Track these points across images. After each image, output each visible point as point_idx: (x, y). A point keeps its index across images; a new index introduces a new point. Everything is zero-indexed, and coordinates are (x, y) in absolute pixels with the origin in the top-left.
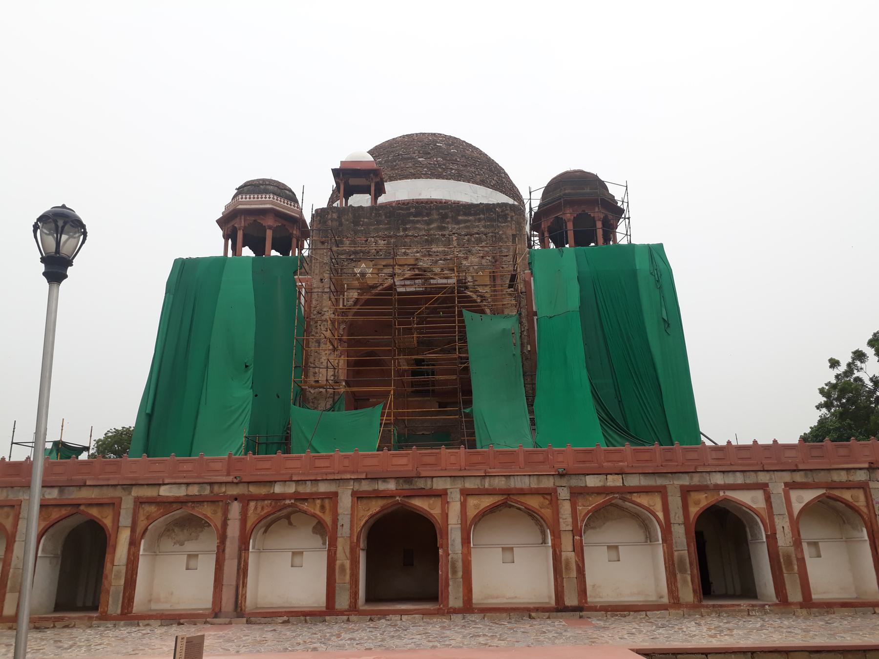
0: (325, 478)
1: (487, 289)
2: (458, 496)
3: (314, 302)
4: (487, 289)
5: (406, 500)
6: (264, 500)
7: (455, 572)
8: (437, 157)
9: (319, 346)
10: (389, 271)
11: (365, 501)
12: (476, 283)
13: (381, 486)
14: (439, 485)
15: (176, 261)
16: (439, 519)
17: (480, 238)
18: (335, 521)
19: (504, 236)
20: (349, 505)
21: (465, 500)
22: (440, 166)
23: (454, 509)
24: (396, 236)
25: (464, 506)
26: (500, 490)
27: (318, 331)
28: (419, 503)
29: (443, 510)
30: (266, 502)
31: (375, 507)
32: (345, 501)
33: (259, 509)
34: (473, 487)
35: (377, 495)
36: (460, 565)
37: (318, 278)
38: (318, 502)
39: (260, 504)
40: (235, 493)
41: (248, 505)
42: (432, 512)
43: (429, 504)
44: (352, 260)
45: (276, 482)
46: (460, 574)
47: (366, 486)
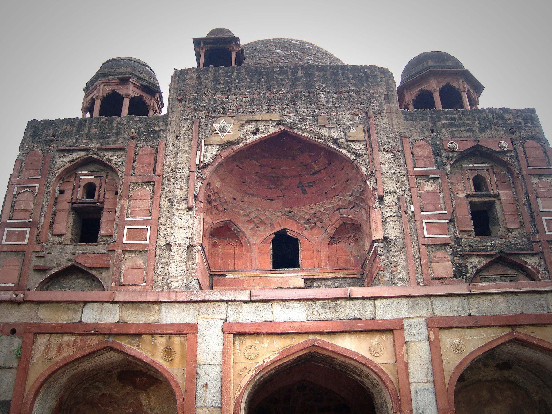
0: (173, 298)
2: (424, 331)
3: (168, 160)
4: (361, 146)
5: (325, 339)
6: (62, 334)
8: (294, 49)
9: (171, 205)
10: (252, 127)
11: (248, 342)
12: (349, 139)
15: (30, 123)
16: (389, 372)
17: (350, 95)
18: (192, 376)
19: (375, 95)
20: (219, 348)
21: (437, 338)
22: (297, 56)
24: (259, 93)
25: (435, 348)
26: (495, 318)
27: (171, 189)
28: (348, 344)
29: (396, 355)
30: (66, 338)
31: (269, 352)
33: (54, 351)
34: (449, 314)
37: (173, 135)
38: (161, 341)
39: (55, 340)
40: (12, 321)
41: (34, 341)
42: (377, 361)
43: (371, 347)
44: (211, 116)
45: (85, 303)
47: (250, 315)
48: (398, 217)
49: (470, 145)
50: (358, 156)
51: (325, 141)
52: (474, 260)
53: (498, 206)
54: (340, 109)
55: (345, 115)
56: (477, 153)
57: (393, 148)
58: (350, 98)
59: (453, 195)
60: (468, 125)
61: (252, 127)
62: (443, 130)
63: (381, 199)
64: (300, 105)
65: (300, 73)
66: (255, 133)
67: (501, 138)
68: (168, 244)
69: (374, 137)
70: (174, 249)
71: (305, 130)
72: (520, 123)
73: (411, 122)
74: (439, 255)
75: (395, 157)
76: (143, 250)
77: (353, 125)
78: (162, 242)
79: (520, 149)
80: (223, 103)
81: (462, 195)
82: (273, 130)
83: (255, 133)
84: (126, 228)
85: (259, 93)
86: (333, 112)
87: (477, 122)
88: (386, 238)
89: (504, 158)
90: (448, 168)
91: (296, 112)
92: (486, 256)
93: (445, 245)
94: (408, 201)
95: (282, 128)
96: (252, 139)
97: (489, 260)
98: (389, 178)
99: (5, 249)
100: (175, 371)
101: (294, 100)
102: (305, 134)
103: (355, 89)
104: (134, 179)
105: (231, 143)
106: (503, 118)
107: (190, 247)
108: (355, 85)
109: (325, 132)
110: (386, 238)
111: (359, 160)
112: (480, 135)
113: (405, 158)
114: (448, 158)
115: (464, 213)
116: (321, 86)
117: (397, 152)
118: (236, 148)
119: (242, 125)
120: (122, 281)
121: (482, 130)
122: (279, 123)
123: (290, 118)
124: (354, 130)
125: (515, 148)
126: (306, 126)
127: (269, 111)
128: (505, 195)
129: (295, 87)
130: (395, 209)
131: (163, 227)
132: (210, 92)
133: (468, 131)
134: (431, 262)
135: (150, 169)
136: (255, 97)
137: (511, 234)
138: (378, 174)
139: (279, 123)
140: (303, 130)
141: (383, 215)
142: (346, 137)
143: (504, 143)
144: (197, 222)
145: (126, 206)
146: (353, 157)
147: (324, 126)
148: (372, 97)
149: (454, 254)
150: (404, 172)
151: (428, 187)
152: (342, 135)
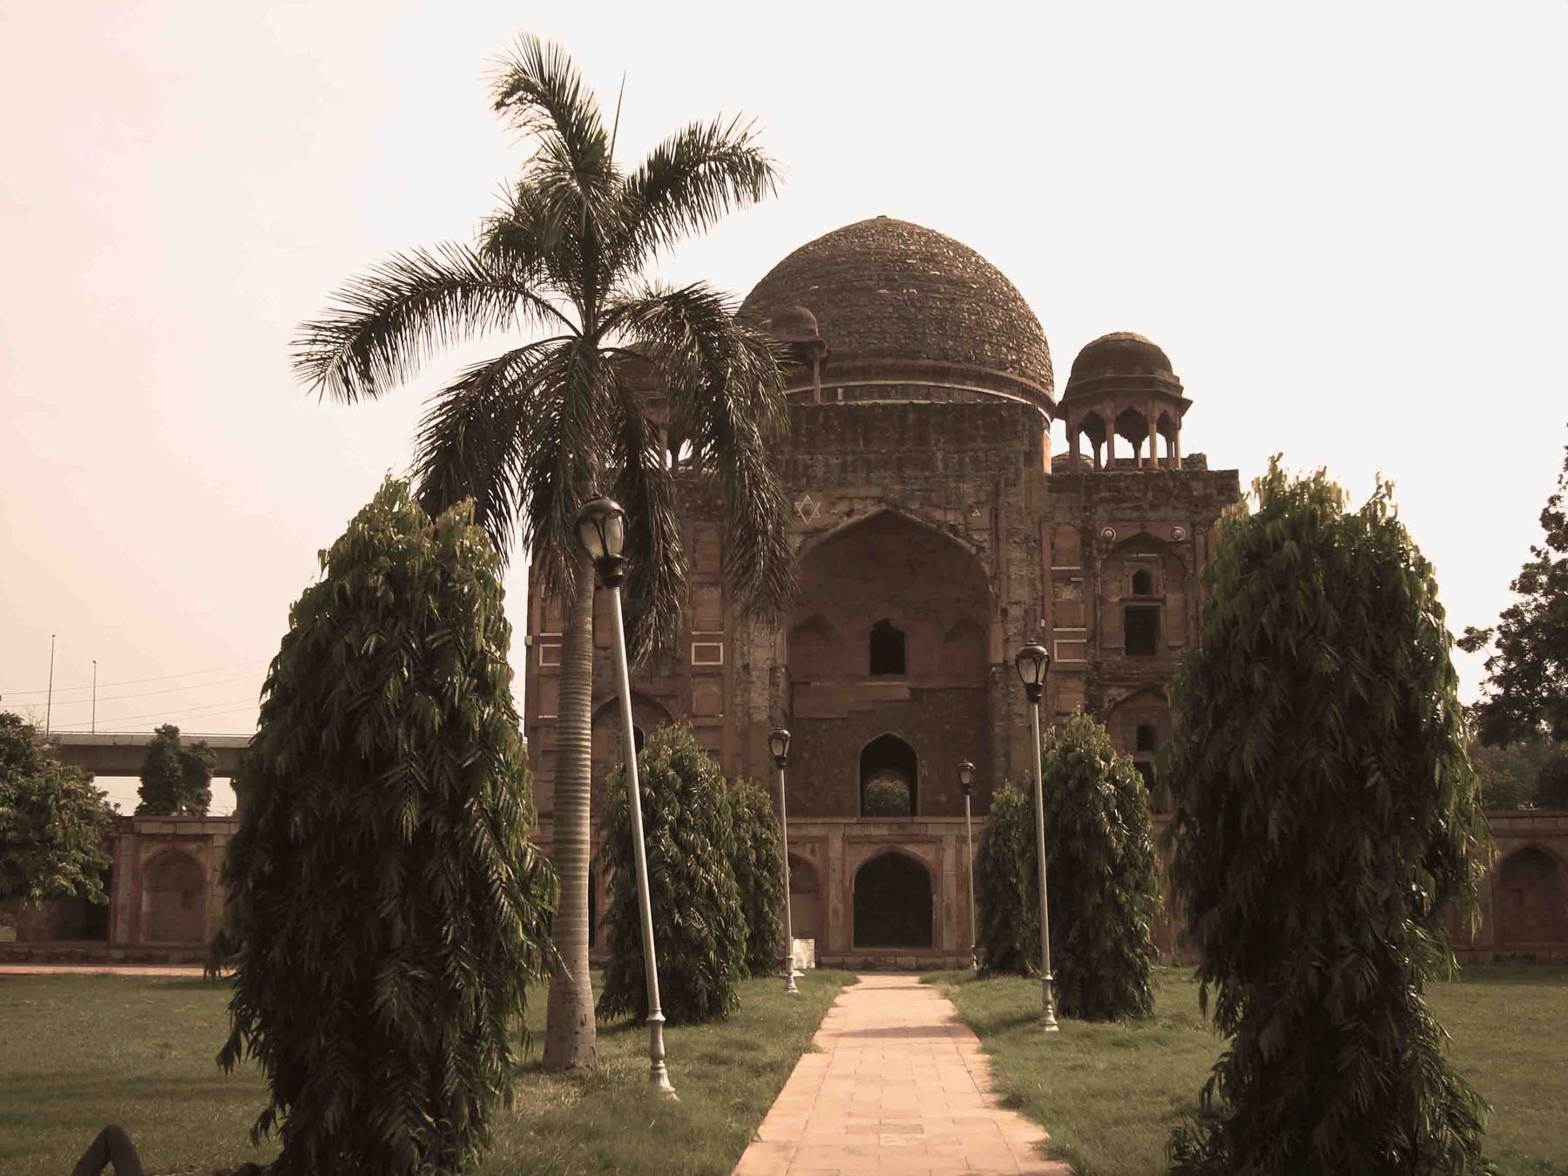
7: (949, 917)
10: (844, 506)
13: (874, 831)
14: (933, 831)
22: (913, 305)
28: (912, 849)
31: (868, 852)
32: (836, 845)
35: (869, 840)
36: (954, 908)
46: (954, 920)
48: (1024, 635)
50: (980, 549)
51: (939, 527)
52: (1113, 692)
54: (960, 478)
55: (967, 488)
56: (1143, 541)
57: (1027, 539)
58: (975, 460)
59: (1102, 600)
60: (1137, 499)
61: (844, 506)
62: (1100, 509)
63: (1005, 612)
64: (908, 472)
65: (911, 417)
66: (849, 514)
67: (1179, 522)
68: (746, 667)
69: (1003, 524)
70: (754, 674)
71: (914, 511)
73: (1055, 495)
74: (1070, 684)
75: (1030, 552)
76: (716, 673)
77: (978, 504)
78: (739, 664)
79: (1201, 539)
80: (807, 467)
81: (1115, 599)
82: (873, 510)
83: (849, 514)
85: (853, 453)
86: (953, 485)
87: (1150, 494)
88: (1006, 662)
89: (1179, 551)
91: (903, 483)
92: (1128, 687)
93: (1078, 673)
94: (1039, 613)
95: (884, 507)
97: (1132, 691)
99: (544, 672)
100: (816, 861)
101: (900, 465)
104: (697, 578)
105: (817, 531)
106: (1188, 488)
107: (773, 670)
108: (984, 439)
109: (938, 515)
110: (1006, 662)
112: (1150, 515)
113: (1041, 552)
114: (1100, 551)
115: (1114, 623)
117: (1033, 546)
118: (825, 535)
119: (833, 504)
122: (880, 500)
124: (977, 513)
126: (915, 506)
127: (868, 481)
128: (1173, 599)
130: (1020, 624)
131: (738, 644)
132: (787, 448)
133: (1136, 508)
135: (715, 564)
136: (849, 458)
137: (1173, 654)
138: (1003, 578)
139: (880, 500)
140: (911, 511)
141: (1005, 632)
142: (967, 524)
143: (1179, 531)
144: (779, 639)
145: (690, 613)
146: (974, 550)
147: (939, 506)
148: (1007, 458)
149: (1089, 683)
150: (1037, 573)
151: (1068, 594)
152: (961, 520)
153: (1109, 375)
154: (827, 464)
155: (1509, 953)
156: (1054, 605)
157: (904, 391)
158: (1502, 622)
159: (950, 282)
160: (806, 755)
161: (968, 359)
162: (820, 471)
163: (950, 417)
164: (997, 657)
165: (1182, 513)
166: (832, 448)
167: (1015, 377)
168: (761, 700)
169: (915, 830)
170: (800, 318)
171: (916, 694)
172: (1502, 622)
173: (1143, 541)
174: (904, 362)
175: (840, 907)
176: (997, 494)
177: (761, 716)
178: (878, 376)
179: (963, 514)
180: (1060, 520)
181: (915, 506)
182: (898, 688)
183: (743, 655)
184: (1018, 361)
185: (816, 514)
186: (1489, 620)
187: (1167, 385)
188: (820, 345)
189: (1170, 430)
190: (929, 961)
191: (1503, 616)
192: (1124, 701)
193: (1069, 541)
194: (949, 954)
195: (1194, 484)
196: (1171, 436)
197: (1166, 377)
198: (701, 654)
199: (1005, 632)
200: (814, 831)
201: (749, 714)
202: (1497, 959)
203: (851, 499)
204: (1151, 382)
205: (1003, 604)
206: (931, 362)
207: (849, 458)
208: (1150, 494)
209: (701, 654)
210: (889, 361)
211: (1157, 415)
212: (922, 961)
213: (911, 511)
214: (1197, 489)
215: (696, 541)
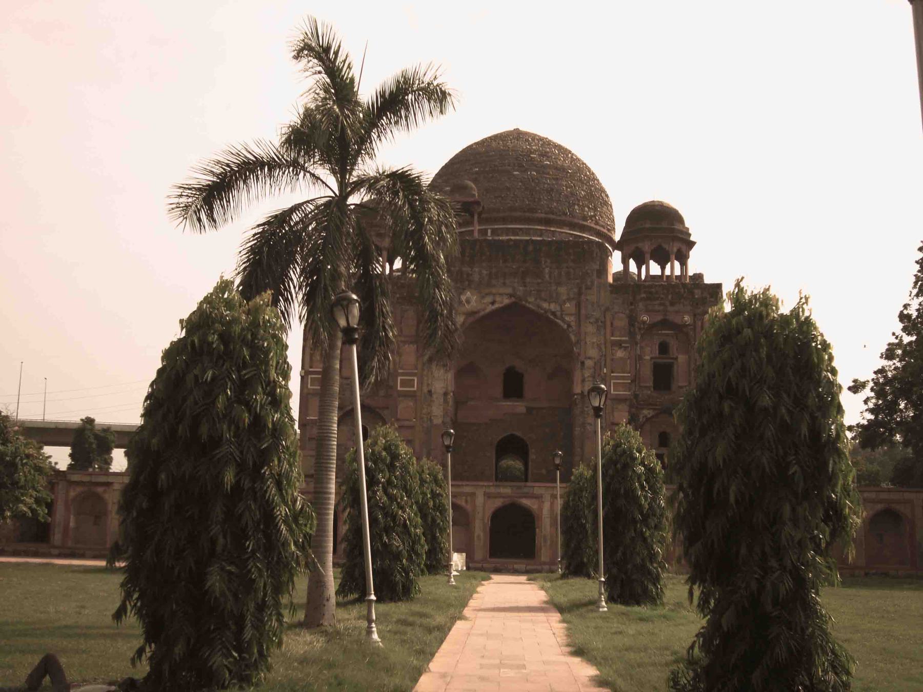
1: (572, 318)
4: (572, 318)
7: (545, 541)
10: (489, 299)
14: (537, 491)
23: (546, 506)
28: (526, 502)
31: (498, 503)
32: (480, 499)
35: (499, 496)
46: (549, 542)
48: (594, 377)
49: (659, 318)
50: (569, 326)
52: (645, 412)
53: (675, 367)
54: (559, 284)
55: (562, 290)
56: (665, 323)
57: (597, 320)
58: (568, 274)
59: (640, 358)
61: (489, 299)
63: (583, 363)
64: (528, 280)
65: (531, 248)
66: (493, 303)
68: (430, 392)
69: (583, 312)
70: (434, 396)
71: (531, 302)
72: (706, 298)
73: (614, 296)
74: (620, 407)
75: (598, 329)
76: (412, 395)
77: (569, 300)
78: (425, 389)
80: (468, 275)
81: (648, 358)
82: (507, 301)
83: (493, 303)
84: (399, 378)
86: (554, 288)
87: (670, 297)
90: (639, 337)
91: (525, 286)
92: (654, 409)
93: (626, 400)
95: (513, 299)
96: (490, 308)
98: (591, 347)
100: (469, 507)
102: (531, 306)
103: (571, 264)
104: (403, 339)
105: (473, 313)
106: (692, 294)
107: (446, 394)
109: (545, 305)
111: (570, 330)
112: (670, 309)
113: (605, 328)
114: (640, 329)
115: (647, 372)
116: (546, 262)
118: (477, 316)
119: (483, 297)
120: (399, 416)
121: (672, 304)
122: (511, 296)
123: (520, 290)
124: (568, 305)
125: (695, 322)
126: (531, 299)
128: (682, 358)
129: (525, 261)
130: (592, 370)
133: (661, 304)
134: (613, 411)
138: (583, 343)
139: (511, 296)
140: (529, 303)
142: (562, 310)
143: (686, 318)
145: (397, 359)
146: (565, 327)
147: (545, 300)
149: (631, 406)
151: (620, 354)
152: (558, 308)
153: (648, 226)
154: (480, 273)
155: (874, 571)
156: (612, 360)
157: (527, 232)
158: (874, 376)
159: (556, 168)
160: (464, 445)
161: (565, 214)
162: (476, 277)
163: (553, 248)
164: (577, 389)
165: (689, 308)
166: (484, 264)
167: (593, 225)
168: (438, 412)
169: (526, 490)
170: (465, 188)
171: (529, 410)
172: (874, 376)
173: (665, 323)
174: (527, 214)
175: (482, 535)
176: (580, 294)
177: (438, 421)
178: (511, 222)
179: (560, 305)
180: (616, 308)
181: (531, 299)
182: (520, 407)
183: (428, 385)
184: (595, 216)
185: (473, 303)
186: (867, 375)
187: (682, 232)
188: (477, 203)
189: (683, 259)
190: (535, 567)
191: (875, 373)
192: (653, 417)
193: (622, 322)
194: (545, 563)
195: (696, 291)
196: (684, 264)
197: (681, 227)
198: (404, 383)
199: (583, 375)
200: (468, 490)
201: (431, 420)
202: (866, 574)
203: (494, 295)
204: (673, 230)
205: (582, 358)
206: (543, 215)
207: (494, 270)
208: (670, 297)
209: (404, 383)
210: (518, 214)
211: (675, 250)
212: (529, 567)
213: (529, 303)
214: (698, 293)
215: (402, 317)
